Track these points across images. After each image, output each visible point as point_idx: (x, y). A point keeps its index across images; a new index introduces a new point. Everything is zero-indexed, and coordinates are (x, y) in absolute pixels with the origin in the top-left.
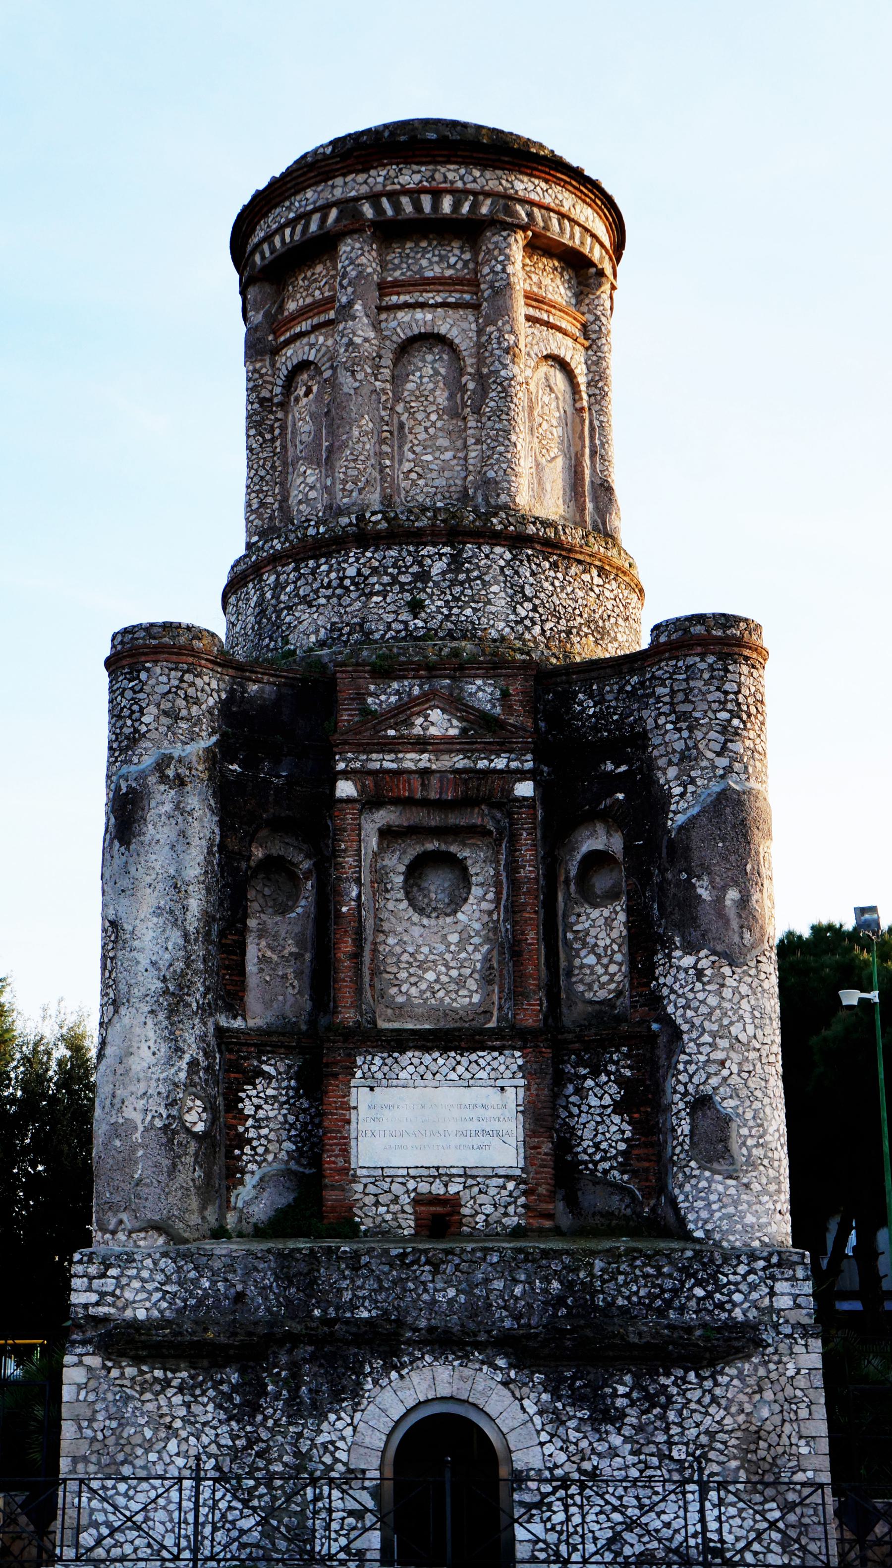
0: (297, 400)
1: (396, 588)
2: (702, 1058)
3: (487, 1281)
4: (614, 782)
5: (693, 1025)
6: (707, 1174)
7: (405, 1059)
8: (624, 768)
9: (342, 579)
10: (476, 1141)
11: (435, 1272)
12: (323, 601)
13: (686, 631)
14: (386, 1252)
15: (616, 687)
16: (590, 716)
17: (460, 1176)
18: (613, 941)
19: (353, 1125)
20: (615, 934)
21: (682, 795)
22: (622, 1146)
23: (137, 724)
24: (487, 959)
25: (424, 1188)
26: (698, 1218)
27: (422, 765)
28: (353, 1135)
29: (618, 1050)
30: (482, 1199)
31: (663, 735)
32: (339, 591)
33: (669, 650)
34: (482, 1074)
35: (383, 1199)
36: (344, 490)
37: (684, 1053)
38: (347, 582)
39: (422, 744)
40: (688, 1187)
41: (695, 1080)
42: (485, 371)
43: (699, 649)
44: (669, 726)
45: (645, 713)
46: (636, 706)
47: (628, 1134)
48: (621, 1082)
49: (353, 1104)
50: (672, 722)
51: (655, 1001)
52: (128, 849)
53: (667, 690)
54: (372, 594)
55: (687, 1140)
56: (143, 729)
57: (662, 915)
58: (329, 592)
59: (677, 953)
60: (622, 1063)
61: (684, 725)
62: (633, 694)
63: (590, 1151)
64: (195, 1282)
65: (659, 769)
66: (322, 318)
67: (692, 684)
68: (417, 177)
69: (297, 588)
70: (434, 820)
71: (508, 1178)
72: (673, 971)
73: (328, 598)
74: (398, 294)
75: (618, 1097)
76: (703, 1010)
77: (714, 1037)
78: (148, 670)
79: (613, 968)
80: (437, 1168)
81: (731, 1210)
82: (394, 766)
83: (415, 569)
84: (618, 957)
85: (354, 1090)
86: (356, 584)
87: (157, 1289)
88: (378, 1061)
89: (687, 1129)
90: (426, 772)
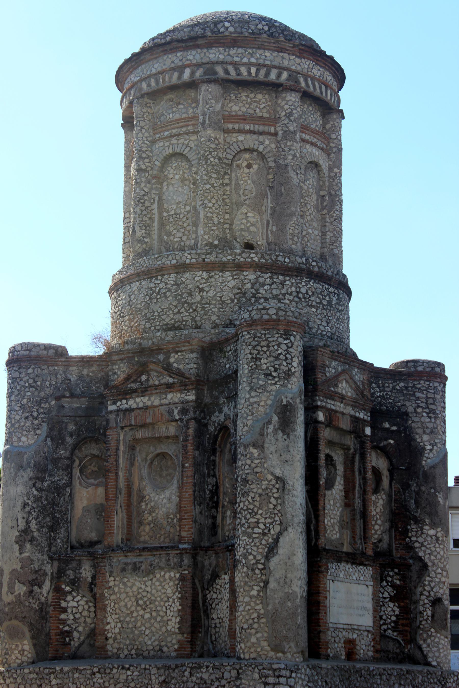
0: (239, 166)
1: (321, 306)
2: (437, 580)
3: (394, 684)
5: (434, 564)
6: (439, 635)
8: (394, 428)
9: (298, 293)
10: (361, 612)
11: (381, 679)
12: (288, 302)
13: (433, 369)
14: (369, 668)
15: (391, 385)
16: (378, 397)
18: (377, 513)
20: (378, 510)
21: (431, 450)
22: (394, 618)
23: (290, 366)
24: (341, 516)
26: (434, 656)
27: (342, 410)
29: (392, 570)
31: (420, 418)
32: (296, 299)
33: (427, 377)
35: (337, 640)
36: (293, 240)
37: (429, 576)
38: (301, 295)
39: (342, 398)
40: (429, 641)
41: (434, 590)
42: (333, 193)
43: (439, 380)
44: (424, 414)
45: (408, 403)
46: (402, 398)
47: (397, 613)
48: (393, 586)
50: (426, 413)
51: (410, 548)
52: (288, 437)
53: (424, 396)
55: (430, 618)
56: (293, 370)
57: (417, 507)
58: (291, 298)
59: (427, 527)
60: (395, 577)
61: (432, 416)
62: (401, 391)
64: (317, 681)
65: (417, 434)
66: (266, 129)
67: (436, 396)
69: (271, 289)
72: (424, 536)
73: (291, 301)
74: (305, 133)
75: (392, 594)
77: (442, 570)
78: (294, 336)
81: (445, 653)
82: (333, 407)
84: (379, 522)
86: (305, 298)
87: (307, 685)
89: (430, 613)
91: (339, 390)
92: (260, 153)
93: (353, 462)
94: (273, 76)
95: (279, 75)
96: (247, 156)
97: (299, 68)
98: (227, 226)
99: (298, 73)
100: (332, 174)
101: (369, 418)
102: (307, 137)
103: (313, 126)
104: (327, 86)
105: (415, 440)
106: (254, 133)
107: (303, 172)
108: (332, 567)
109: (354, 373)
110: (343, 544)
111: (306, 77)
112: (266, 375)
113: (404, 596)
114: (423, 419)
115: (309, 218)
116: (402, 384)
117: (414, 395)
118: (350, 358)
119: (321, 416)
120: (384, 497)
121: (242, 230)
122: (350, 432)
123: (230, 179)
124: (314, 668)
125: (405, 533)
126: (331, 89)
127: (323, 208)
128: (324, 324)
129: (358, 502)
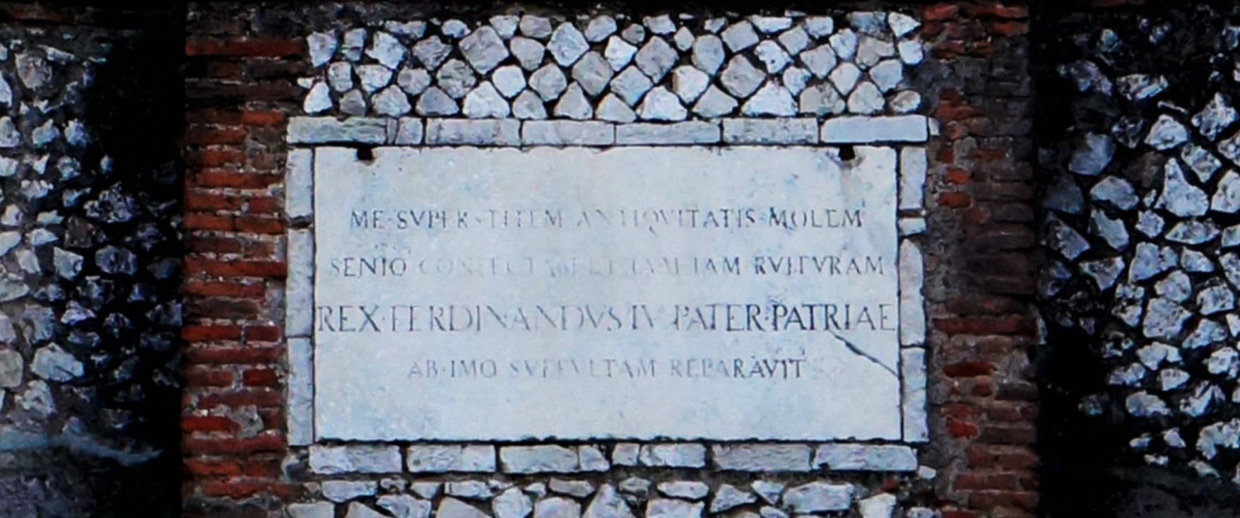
7: (488, 40)
10: (751, 345)
17: (690, 474)
19: (296, 286)
28: (296, 322)
34: (772, 99)
49: (295, 209)
63: (1171, 380)
71: (868, 480)
80: (607, 446)
85: (298, 158)
88: (386, 49)
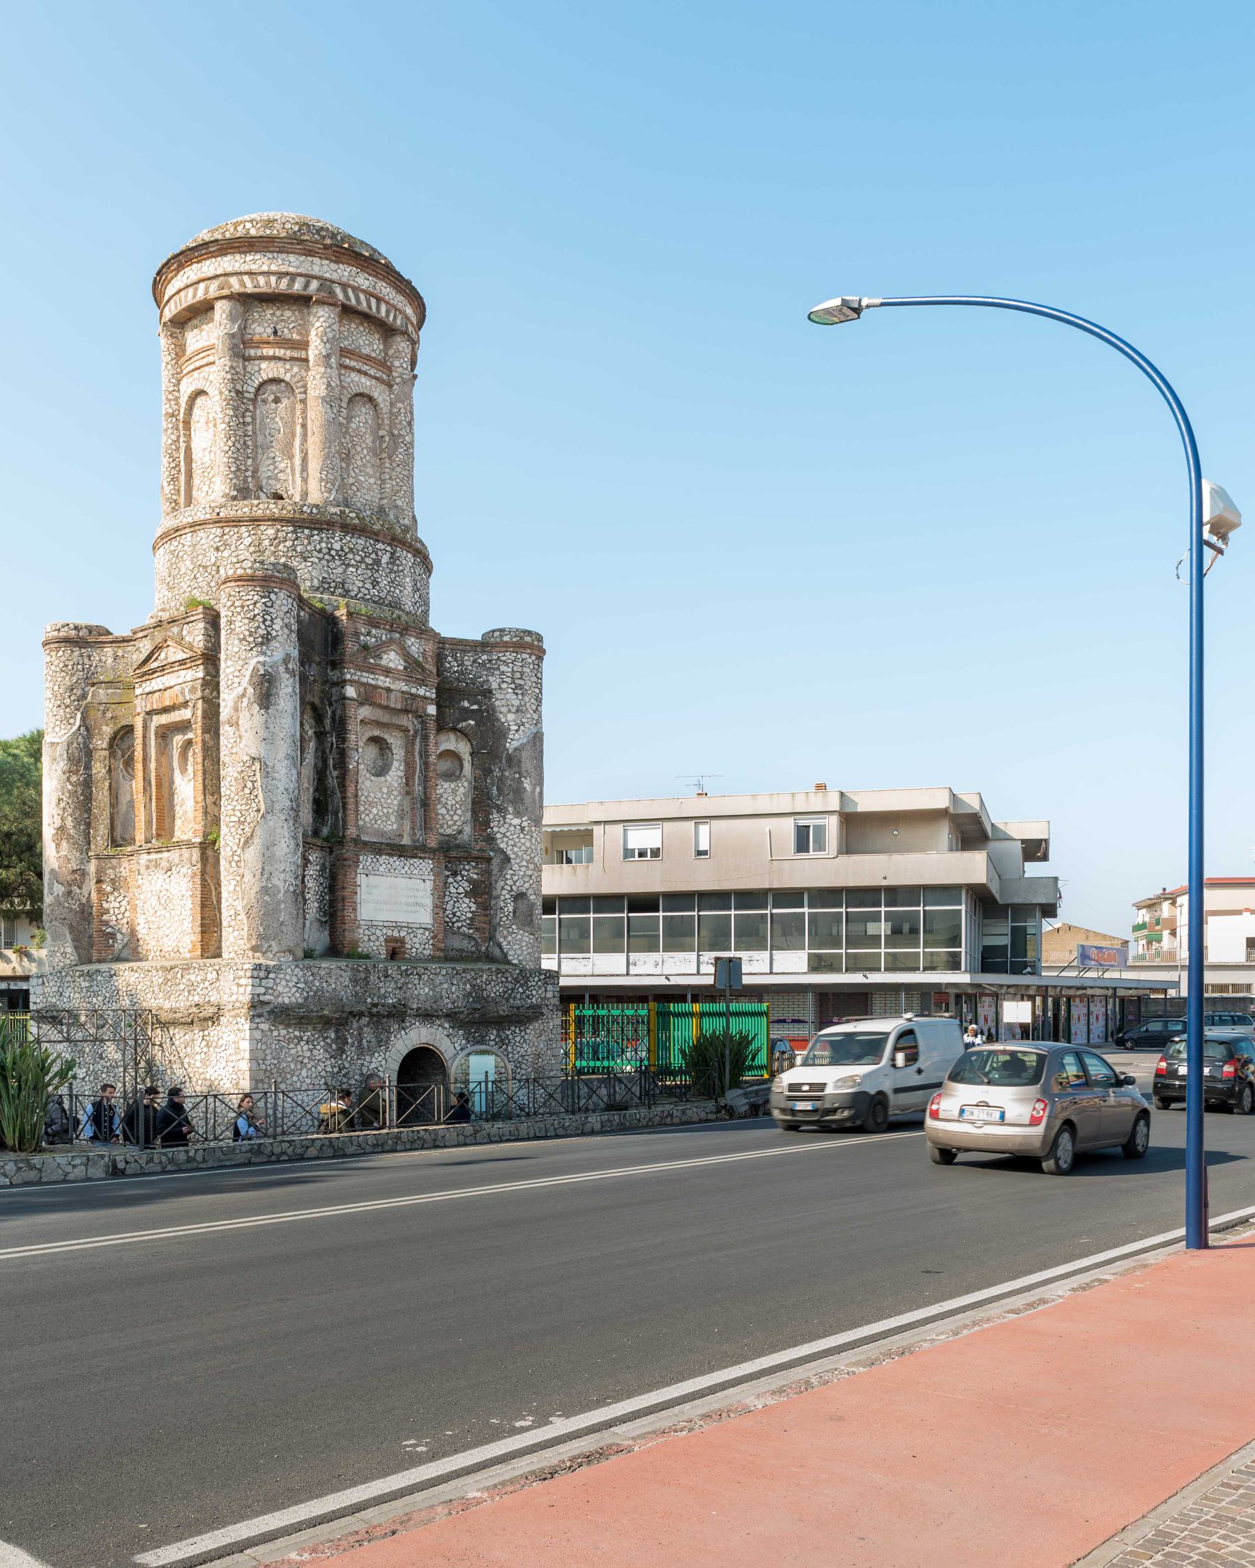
1: (363, 566)
4: (467, 714)
8: (475, 707)
9: (330, 549)
10: (413, 909)
20: (458, 799)
21: (517, 731)
24: (401, 805)
25: (390, 933)
27: (387, 685)
30: (415, 940)
34: (415, 872)
38: (333, 553)
39: (387, 672)
42: (396, 432)
45: (491, 679)
51: (491, 839)
54: (348, 565)
57: (500, 794)
58: (320, 555)
59: (510, 816)
62: (483, 664)
68: (367, 283)
70: (384, 717)
73: (320, 559)
76: (523, 848)
79: (456, 818)
82: (373, 682)
83: (373, 556)
89: (511, 909)
90: (388, 690)
91: (384, 662)
92: (287, 383)
93: (413, 744)
94: (298, 286)
95: (307, 285)
96: (274, 387)
97: (335, 276)
98: (249, 473)
99: (333, 282)
100: (395, 410)
101: (434, 696)
102: (353, 364)
103: (366, 350)
104: (379, 300)
105: (499, 720)
106: (280, 359)
107: (344, 405)
108: (366, 860)
109: (409, 643)
110: (401, 836)
111: (344, 286)
112: (241, 640)
113: (482, 892)
114: (508, 696)
115: (359, 463)
116: (485, 657)
117: (498, 669)
118: (420, 626)
119: (350, 692)
120: (466, 784)
121: (269, 478)
122: (406, 711)
123: (254, 418)
124: (309, 968)
125: (487, 823)
126: (387, 303)
127: (382, 451)
128: (368, 586)
129: (418, 789)
